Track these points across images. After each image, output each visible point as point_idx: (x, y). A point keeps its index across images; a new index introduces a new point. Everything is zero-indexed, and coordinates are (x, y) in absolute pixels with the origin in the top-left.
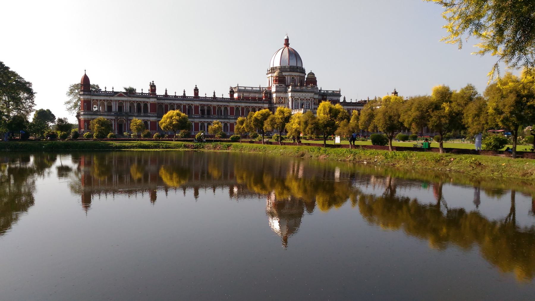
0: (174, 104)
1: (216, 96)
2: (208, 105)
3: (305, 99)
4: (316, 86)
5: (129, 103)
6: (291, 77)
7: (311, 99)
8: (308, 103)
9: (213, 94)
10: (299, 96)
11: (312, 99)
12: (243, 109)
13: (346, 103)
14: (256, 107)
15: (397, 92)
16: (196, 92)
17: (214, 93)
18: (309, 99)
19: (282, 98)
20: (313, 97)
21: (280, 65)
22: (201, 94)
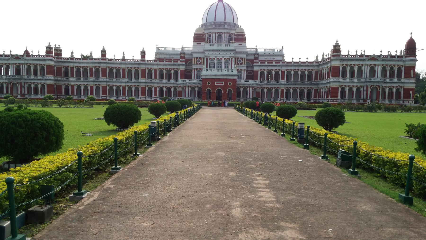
0: (80, 67)
1: (126, 58)
2: (116, 67)
3: (223, 59)
4: (243, 44)
5: (25, 66)
6: (216, 34)
7: (230, 59)
8: (228, 64)
9: (123, 55)
10: (215, 55)
11: (232, 59)
12: (156, 71)
13: (286, 63)
14: (171, 69)
15: (339, 44)
16: (104, 53)
17: (124, 54)
18: (229, 59)
19: (200, 58)
20: (233, 56)
21: (207, 22)
22: (109, 56)
